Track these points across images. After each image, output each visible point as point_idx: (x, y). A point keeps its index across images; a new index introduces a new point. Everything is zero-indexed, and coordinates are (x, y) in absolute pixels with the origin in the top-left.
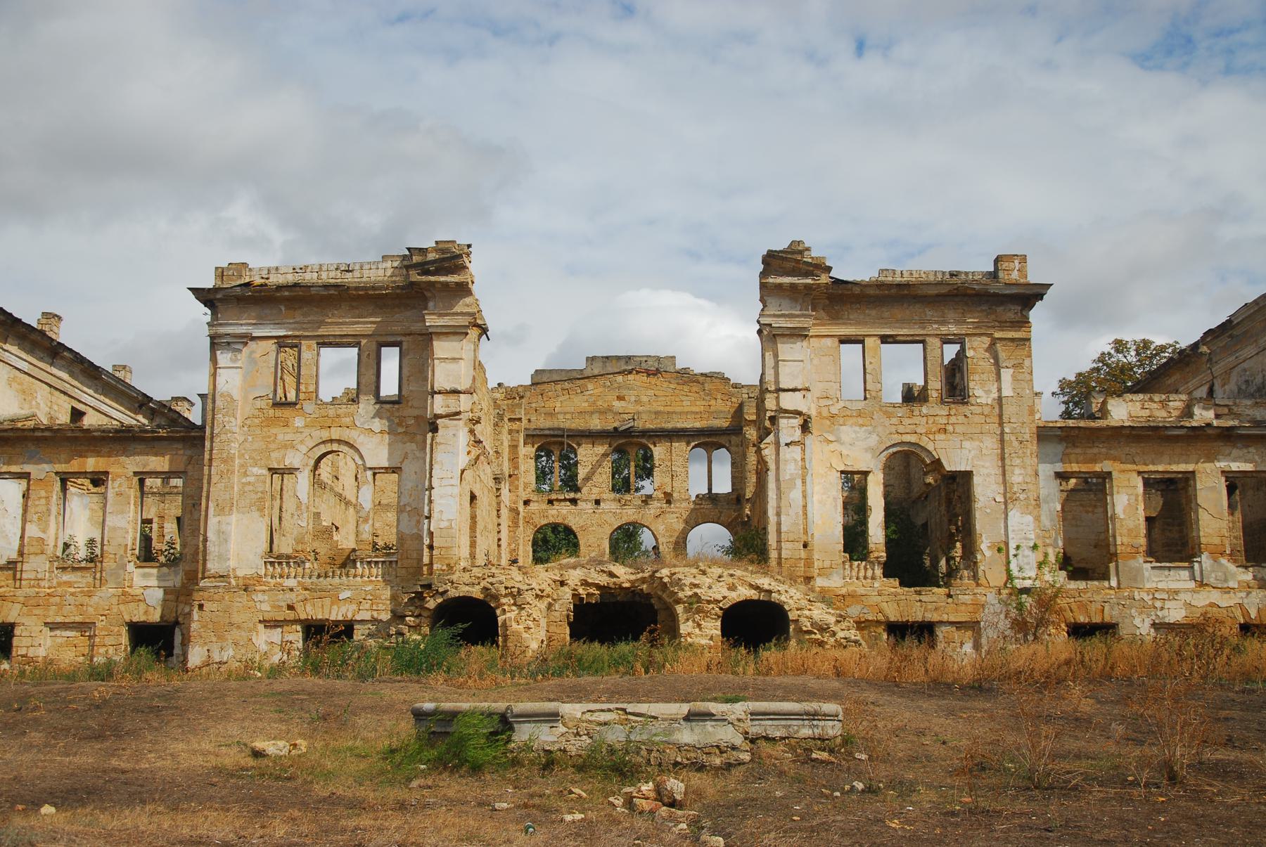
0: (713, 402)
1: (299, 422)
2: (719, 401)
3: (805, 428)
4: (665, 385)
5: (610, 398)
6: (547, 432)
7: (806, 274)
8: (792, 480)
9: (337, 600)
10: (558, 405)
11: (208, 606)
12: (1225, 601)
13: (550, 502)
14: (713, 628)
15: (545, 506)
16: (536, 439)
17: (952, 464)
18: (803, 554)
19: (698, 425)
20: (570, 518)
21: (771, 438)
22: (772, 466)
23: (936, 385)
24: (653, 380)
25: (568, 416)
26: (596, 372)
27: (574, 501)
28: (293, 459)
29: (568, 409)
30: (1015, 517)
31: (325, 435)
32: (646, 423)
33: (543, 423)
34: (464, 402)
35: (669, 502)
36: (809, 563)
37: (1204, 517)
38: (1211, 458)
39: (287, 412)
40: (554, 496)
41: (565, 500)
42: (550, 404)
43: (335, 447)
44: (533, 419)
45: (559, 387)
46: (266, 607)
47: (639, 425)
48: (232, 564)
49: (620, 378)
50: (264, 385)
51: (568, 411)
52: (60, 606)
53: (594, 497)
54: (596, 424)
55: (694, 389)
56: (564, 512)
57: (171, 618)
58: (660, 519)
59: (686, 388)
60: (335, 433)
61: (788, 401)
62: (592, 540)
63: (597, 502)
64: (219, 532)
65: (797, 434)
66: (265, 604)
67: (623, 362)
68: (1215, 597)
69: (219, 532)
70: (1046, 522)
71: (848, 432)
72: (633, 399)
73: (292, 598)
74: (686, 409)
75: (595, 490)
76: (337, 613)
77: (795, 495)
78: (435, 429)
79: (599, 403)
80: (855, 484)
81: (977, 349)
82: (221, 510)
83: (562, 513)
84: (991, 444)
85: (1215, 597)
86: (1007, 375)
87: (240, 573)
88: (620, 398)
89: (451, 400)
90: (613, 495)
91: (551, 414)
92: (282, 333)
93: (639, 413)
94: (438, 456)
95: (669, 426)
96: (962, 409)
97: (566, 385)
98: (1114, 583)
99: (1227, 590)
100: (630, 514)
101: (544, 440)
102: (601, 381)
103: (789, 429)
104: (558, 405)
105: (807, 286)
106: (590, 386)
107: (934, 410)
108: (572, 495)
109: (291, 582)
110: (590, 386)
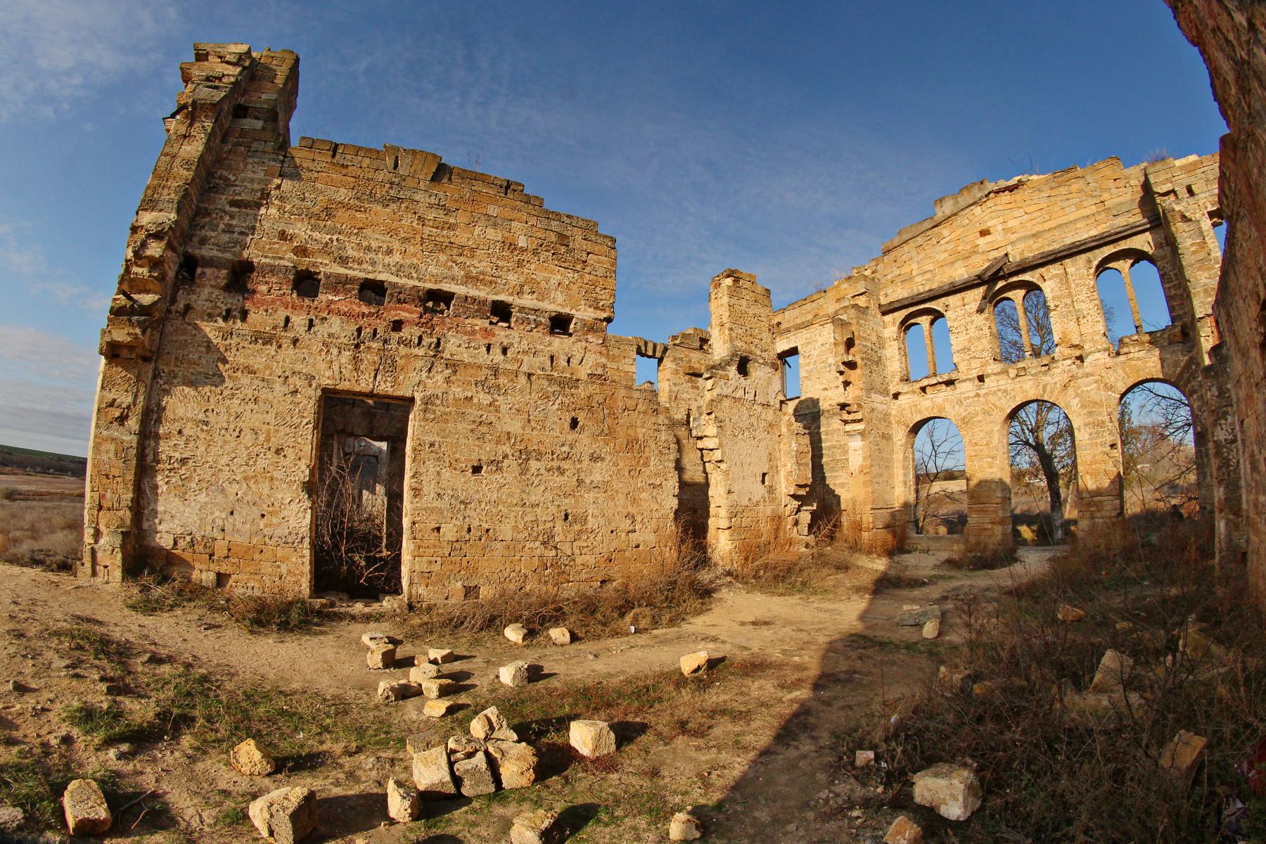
0: (1105, 196)
2: (1114, 191)
10: (914, 266)
15: (916, 398)
19: (1094, 232)
25: (929, 275)
27: (950, 383)
29: (927, 268)
33: (899, 293)
40: (925, 383)
42: (905, 270)
44: (889, 292)
45: (912, 244)
47: (1015, 256)
53: (975, 373)
54: (961, 273)
56: (939, 400)
58: (1070, 391)
63: (981, 378)
72: (1000, 228)
75: (976, 364)
79: (960, 248)
88: (984, 233)
90: (997, 367)
91: (909, 279)
93: (1012, 243)
95: (1056, 246)
97: (920, 240)
100: (1028, 388)
101: (904, 313)
102: (959, 221)
106: (945, 232)
108: (946, 378)
110: (945, 232)
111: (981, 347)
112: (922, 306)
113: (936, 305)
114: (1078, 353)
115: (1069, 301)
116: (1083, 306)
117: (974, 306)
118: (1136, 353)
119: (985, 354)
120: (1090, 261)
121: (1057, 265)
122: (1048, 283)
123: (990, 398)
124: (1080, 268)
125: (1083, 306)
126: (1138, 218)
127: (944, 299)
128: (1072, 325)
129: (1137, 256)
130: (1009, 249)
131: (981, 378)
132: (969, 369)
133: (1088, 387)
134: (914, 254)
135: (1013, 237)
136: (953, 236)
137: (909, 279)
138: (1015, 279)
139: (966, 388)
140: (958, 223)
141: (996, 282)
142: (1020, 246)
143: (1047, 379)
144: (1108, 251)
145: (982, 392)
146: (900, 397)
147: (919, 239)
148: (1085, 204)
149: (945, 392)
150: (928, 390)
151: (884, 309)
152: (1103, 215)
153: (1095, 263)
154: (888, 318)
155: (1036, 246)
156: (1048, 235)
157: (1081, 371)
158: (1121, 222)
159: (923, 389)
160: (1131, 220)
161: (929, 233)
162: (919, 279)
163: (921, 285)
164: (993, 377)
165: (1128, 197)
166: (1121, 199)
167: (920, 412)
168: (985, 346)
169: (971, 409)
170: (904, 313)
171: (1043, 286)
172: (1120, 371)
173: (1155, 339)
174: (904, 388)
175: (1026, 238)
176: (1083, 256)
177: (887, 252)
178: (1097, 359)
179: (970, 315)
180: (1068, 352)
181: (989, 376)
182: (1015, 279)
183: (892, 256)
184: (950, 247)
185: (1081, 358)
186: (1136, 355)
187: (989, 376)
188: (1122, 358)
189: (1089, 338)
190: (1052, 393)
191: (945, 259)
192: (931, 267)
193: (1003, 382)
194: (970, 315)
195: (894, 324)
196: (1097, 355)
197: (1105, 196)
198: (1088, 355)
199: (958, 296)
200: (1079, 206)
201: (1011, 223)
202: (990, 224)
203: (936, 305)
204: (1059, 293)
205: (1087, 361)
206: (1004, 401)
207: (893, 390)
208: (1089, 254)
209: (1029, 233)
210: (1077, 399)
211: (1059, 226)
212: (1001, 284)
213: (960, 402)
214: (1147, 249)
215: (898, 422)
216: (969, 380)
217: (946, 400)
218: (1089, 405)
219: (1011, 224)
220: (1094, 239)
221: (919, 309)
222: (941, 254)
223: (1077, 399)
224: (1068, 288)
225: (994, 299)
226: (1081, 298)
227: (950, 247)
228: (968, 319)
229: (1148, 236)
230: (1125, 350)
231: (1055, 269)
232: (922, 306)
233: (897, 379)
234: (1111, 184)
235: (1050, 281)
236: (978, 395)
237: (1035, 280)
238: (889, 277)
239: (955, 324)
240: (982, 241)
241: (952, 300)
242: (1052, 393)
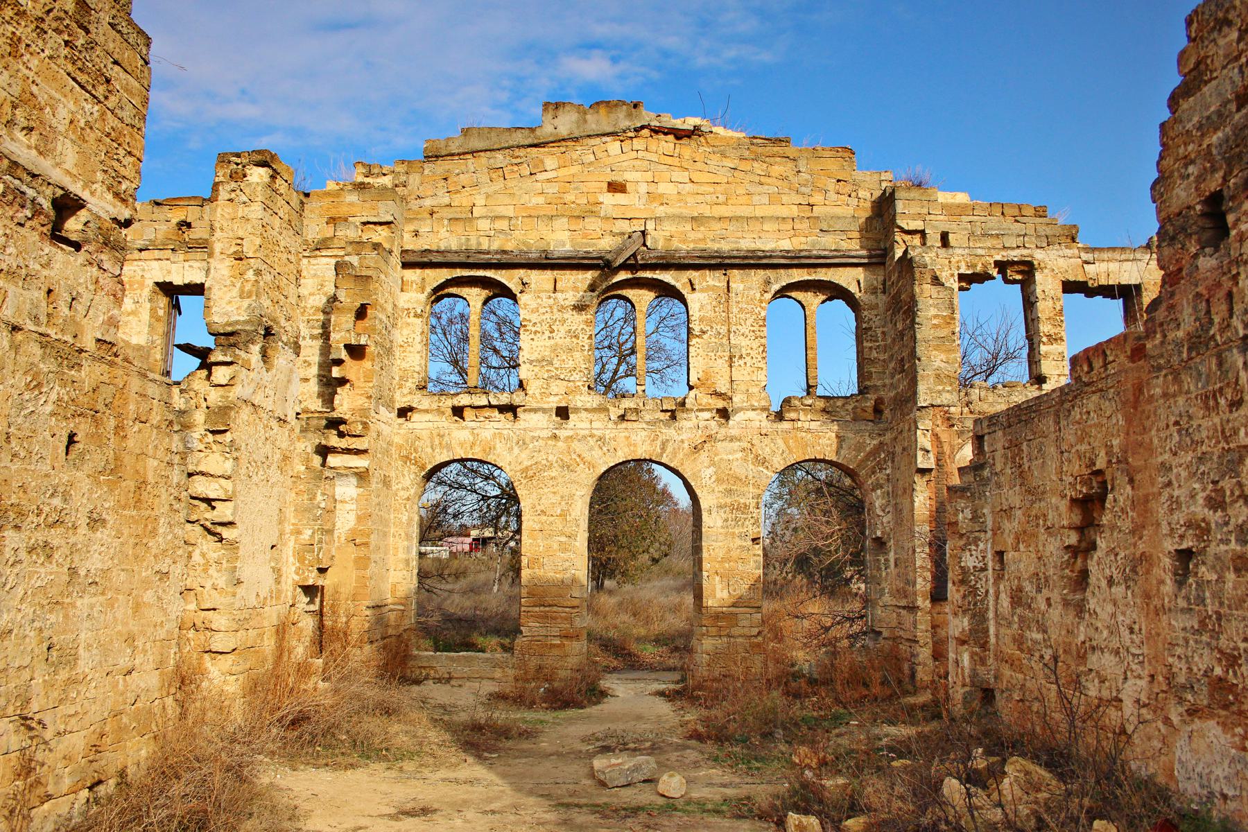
2: (832, 196)
4: (715, 160)
5: (592, 186)
6: (456, 259)
10: (480, 201)
13: (458, 411)
16: (429, 272)
19: (786, 245)
20: (500, 447)
24: (687, 149)
25: (503, 224)
26: (564, 131)
33: (445, 238)
35: (724, 414)
40: (464, 400)
41: (490, 406)
42: (462, 200)
44: (424, 229)
47: (660, 239)
49: (614, 146)
51: (499, 209)
53: (554, 402)
54: (561, 239)
55: (777, 170)
58: (703, 456)
59: (758, 167)
62: (549, 499)
63: (563, 413)
67: (621, 113)
72: (643, 188)
74: (759, 212)
75: (557, 387)
79: (569, 198)
83: (482, 436)
88: (616, 187)
90: (594, 400)
91: (467, 218)
93: (657, 219)
95: (725, 247)
97: (500, 159)
100: (635, 442)
101: (444, 275)
102: (577, 152)
104: (480, 201)
106: (550, 163)
108: (504, 399)
110: (550, 163)
111: (571, 364)
112: (481, 273)
114: (720, 404)
115: (724, 330)
116: (744, 342)
117: (571, 298)
119: (576, 376)
120: (768, 282)
121: (718, 274)
122: (696, 295)
123: (576, 445)
124: (746, 284)
125: (744, 342)
126: (853, 246)
127: (522, 272)
128: (722, 364)
129: (835, 292)
130: (650, 226)
131: (563, 413)
132: (542, 392)
133: (729, 453)
134: (484, 178)
135: (661, 211)
136: (563, 172)
137: (467, 218)
138: (648, 274)
139: (536, 423)
140: (575, 155)
142: (669, 228)
143: (669, 432)
144: (802, 275)
145: (562, 433)
146: (415, 417)
147: (499, 156)
148: (785, 199)
149: (502, 422)
150: (468, 413)
151: (411, 258)
152: (805, 225)
153: (776, 287)
154: (413, 275)
155: (692, 235)
156: (717, 226)
157: (723, 431)
158: (829, 243)
159: (458, 411)
160: (845, 245)
161: (522, 152)
162: (484, 225)
163: (485, 237)
164: (584, 414)
165: (849, 211)
166: (839, 211)
167: (449, 447)
168: (579, 364)
169: (540, 458)
170: (444, 275)
171: (690, 297)
172: (780, 442)
173: (831, 408)
174: (417, 400)
175: (681, 218)
176: (761, 272)
177: (433, 156)
178: (748, 420)
179: (562, 309)
180: (706, 400)
181: (577, 410)
182: (648, 274)
183: (441, 167)
184: (552, 189)
185: (724, 414)
186: (806, 425)
187: (577, 410)
188: (785, 425)
189: (743, 387)
190: (675, 453)
191: (537, 207)
192: (510, 212)
193: (600, 425)
194: (562, 309)
195: (423, 290)
196: (751, 414)
197: (817, 198)
198: (736, 411)
199: (549, 275)
200: (774, 199)
201: (663, 188)
202: (629, 176)
204: (711, 314)
205: (736, 419)
206: (597, 453)
207: (401, 402)
208: (769, 272)
209: (686, 212)
210: (711, 470)
211: (737, 218)
212: (623, 276)
213: (522, 443)
214: (853, 288)
215: (406, 459)
216: (544, 411)
217: (498, 435)
218: (730, 481)
219: (663, 194)
220: (786, 254)
221: (481, 273)
222: (533, 194)
223: (711, 470)
224: (728, 311)
225: (606, 293)
226: (743, 329)
227: (552, 189)
228: (557, 315)
229: (859, 273)
230: (793, 415)
231: (713, 279)
232: (481, 273)
233: (411, 384)
234: (831, 185)
236: (555, 436)
237: (678, 286)
238: (428, 203)
239: (534, 318)
240: (609, 199)
241: (538, 278)
242: (675, 453)
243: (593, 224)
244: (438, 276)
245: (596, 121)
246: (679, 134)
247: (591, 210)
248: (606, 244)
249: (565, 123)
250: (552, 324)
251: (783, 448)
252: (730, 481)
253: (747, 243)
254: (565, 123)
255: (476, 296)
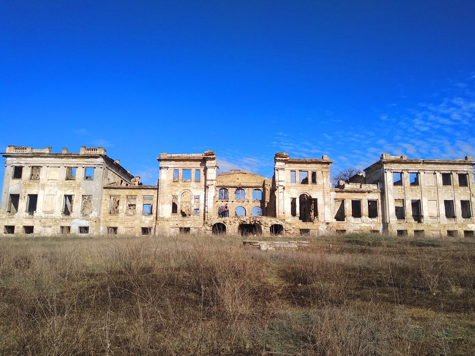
1: (179, 185)
3: (284, 188)
7: (285, 157)
8: (281, 200)
9: (187, 223)
11: (160, 224)
12: (367, 225)
14: (268, 229)
15: (221, 202)
17: (313, 197)
18: (283, 215)
21: (277, 191)
22: (277, 196)
23: (310, 180)
28: (177, 193)
30: (326, 208)
31: (184, 188)
32: (243, 184)
33: (221, 184)
34: (214, 182)
36: (284, 217)
37: (363, 208)
38: (365, 196)
39: (176, 183)
43: (186, 191)
46: (172, 224)
48: (165, 215)
50: (171, 178)
52: (127, 224)
54: (232, 184)
57: (151, 227)
60: (186, 188)
61: (281, 183)
64: (162, 209)
65: (282, 190)
66: (171, 224)
68: (365, 225)
69: (162, 209)
70: (332, 209)
71: (292, 190)
73: (177, 223)
76: (187, 226)
77: (282, 203)
78: (208, 188)
80: (294, 200)
81: (318, 174)
82: (162, 204)
84: (321, 193)
85: (365, 225)
86: (325, 178)
87: (166, 217)
88: (238, 179)
89: (211, 182)
92: (175, 166)
94: (209, 193)
96: (316, 185)
98: (346, 221)
99: (367, 223)
101: (220, 188)
102: (234, 175)
103: (280, 189)
105: (285, 160)
107: (310, 185)
109: (177, 219)
113: (227, 188)
118: (256, 202)
141: (239, 188)
144: (256, 188)
178: (251, 203)
193: (236, 203)
203: (227, 188)
218: (249, 208)
219: (242, 180)
235: (246, 190)
243: (235, 183)
244: (220, 188)
245: (236, 172)
246: (244, 174)
247: (235, 181)
248: (237, 185)
249: (233, 172)
250: (231, 192)
251: (254, 205)
252: (249, 208)
253: (251, 185)
254: (233, 172)
255: (224, 190)
